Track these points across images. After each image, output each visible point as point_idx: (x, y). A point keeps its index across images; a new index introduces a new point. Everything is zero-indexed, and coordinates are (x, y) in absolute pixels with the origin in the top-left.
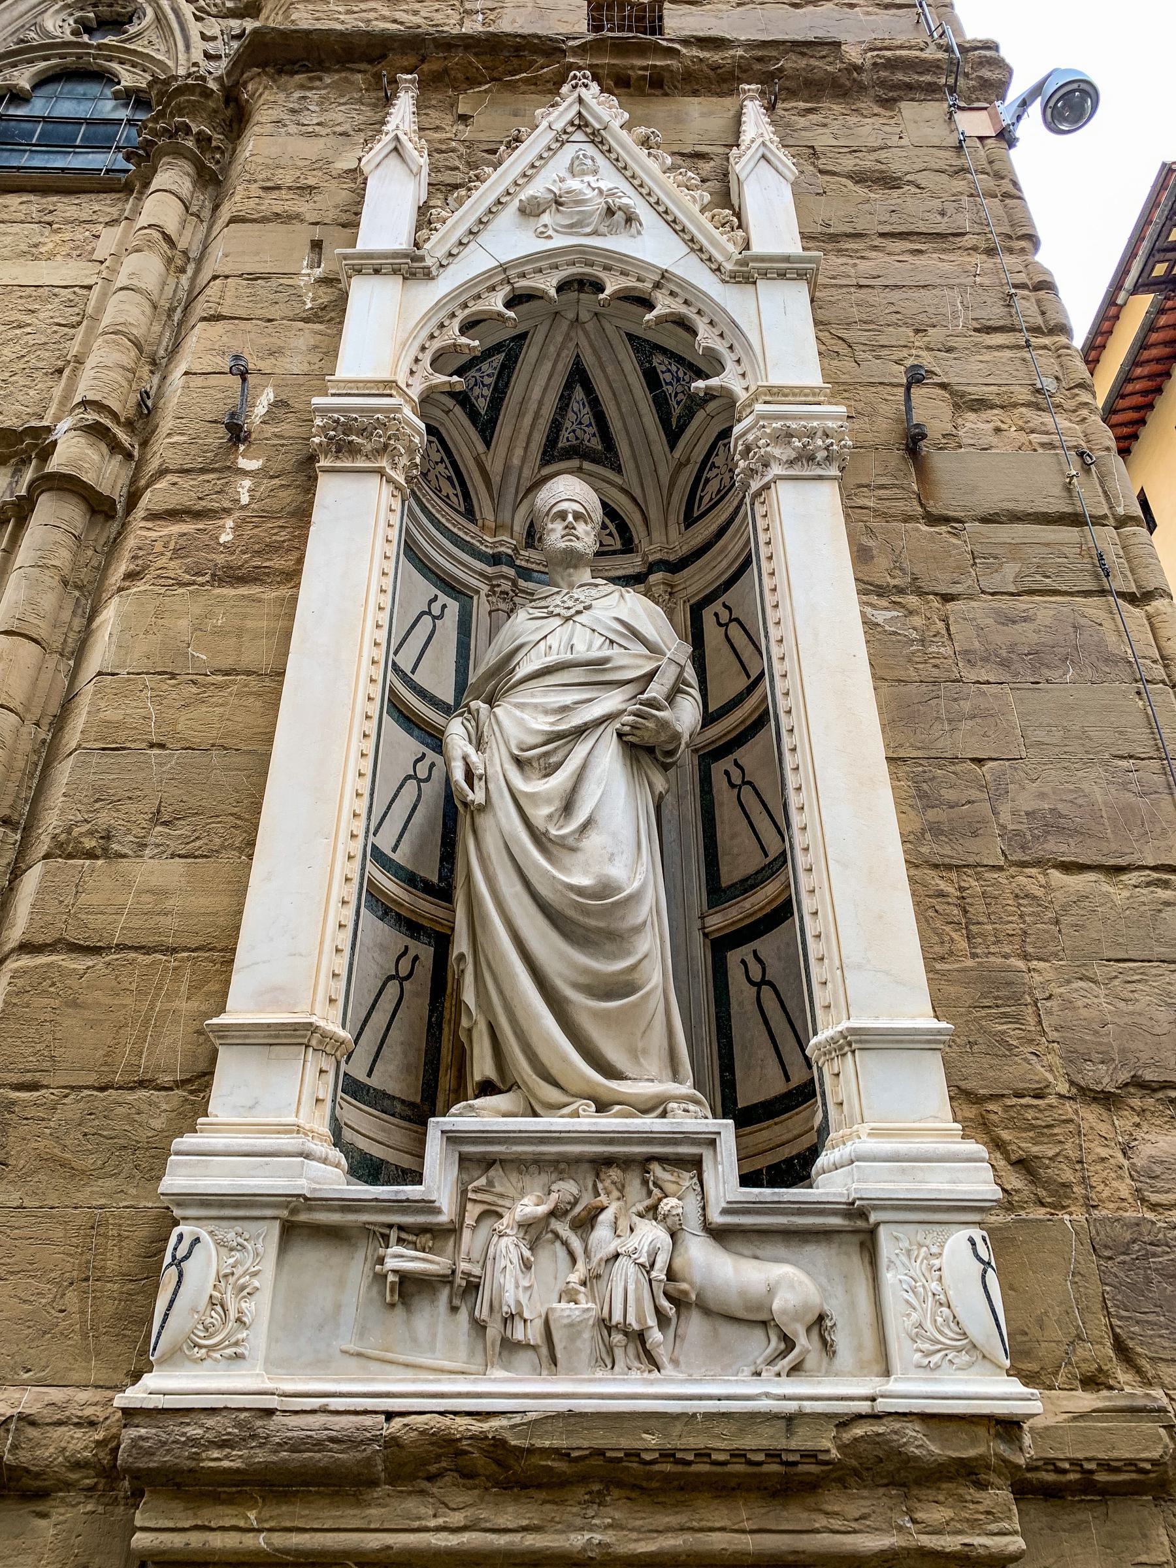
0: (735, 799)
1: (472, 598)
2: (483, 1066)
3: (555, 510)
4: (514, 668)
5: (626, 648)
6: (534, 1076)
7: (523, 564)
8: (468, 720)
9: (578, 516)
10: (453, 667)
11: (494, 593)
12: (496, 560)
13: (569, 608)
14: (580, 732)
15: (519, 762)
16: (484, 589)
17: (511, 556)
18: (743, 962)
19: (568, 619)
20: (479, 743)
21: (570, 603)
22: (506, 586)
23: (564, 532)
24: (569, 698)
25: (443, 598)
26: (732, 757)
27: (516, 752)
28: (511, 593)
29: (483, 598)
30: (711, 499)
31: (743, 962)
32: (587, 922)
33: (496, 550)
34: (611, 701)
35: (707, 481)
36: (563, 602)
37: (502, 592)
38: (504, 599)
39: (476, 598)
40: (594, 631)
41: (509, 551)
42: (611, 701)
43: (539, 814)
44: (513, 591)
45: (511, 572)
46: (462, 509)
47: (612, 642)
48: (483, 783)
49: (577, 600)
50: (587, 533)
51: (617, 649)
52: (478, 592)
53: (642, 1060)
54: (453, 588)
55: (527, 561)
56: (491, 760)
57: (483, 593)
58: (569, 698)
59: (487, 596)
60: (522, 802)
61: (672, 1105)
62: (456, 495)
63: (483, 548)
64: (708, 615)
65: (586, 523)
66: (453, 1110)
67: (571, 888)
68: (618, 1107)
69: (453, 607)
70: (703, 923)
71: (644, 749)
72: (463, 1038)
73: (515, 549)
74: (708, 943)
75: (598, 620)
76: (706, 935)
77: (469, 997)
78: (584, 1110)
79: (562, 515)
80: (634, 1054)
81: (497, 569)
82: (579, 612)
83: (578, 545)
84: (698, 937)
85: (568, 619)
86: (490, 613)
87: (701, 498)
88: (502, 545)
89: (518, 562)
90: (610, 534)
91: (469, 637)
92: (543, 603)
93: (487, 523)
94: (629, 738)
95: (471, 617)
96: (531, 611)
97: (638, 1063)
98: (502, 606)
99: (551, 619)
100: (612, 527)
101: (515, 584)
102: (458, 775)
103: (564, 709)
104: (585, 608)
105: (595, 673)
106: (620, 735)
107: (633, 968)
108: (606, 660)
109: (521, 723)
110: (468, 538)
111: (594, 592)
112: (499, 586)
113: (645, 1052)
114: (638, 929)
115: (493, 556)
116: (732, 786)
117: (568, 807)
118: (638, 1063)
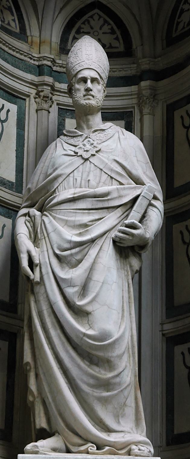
0: (185, 251)
1: (25, 100)
2: (41, 422)
3: (80, 76)
4: (55, 190)
5: (121, 184)
6: (66, 430)
7: (58, 69)
8: (28, 222)
9: (93, 80)
10: (14, 154)
11: (40, 96)
12: (40, 70)
13: (87, 151)
14: (93, 241)
15: (57, 256)
16: (33, 92)
17: (50, 67)
18: (183, 354)
19: (86, 160)
20: (35, 240)
21: (88, 147)
22: (47, 90)
23: (84, 93)
24: (86, 218)
25: (8, 105)
26: (185, 223)
27: (58, 252)
28: (50, 95)
29: (33, 100)
30: (184, 28)
31: (183, 354)
32: (93, 354)
33: (40, 63)
34: (111, 220)
35: (182, 11)
36: (84, 145)
37: (44, 97)
38: (46, 101)
39: (27, 99)
40: (101, 170)
41: (49, 63)
42: (111, 220)
43: (70, 291)
44: (52, 94)
45: (49, 80)
46: (18, 31)
47: (112, 178)
48: (38, 268)
49: (92, 144)
50: (99, 91)
51: (115, 186)
52: (28, 96)
53: (120, 420)
54: (14, 96)
55: (61, 67)
56: (42, 252)
57: (32, 96)
58: (86, 218)
59: (35, 98)
60: (61, 283)
61: (134, 447)
62: (14, 20)
63: (32, 61)
64: (177, 114)
65: (99, 83)
66: (29, 447)
67: (85, 335)
68: (107, 448)
69: (14, 108)
70: (162, 328)
71: (127, 249)
72: (29, 405)
73: (53, 61)
74: (165, 339)
75: (103, 162)
76: (163, 335)
77: (33, 385)
78: (91, 449)
79: (84, 80)
80: (117, 417)
81: (41, 78)
82: (93, 155)
83: (93, 102)
84: (159, 334)
85: (86, 160)
86: (37, 111)
87: (178, 23)
88: (44, 59)
89: (55, 68)
90: (117, 39)
91: (24, 130)
92: (72, 141)
93: (34, 39)
94: (118, 244)
95: (25, 115)
96: (65, 145)
97: (119, 422)
98: (45, 106)
99: (76, 158)
100: (118, 33)
101: (53, 88)
102: (25, 263)
103: (86, 226)
104: (97, 152)
105: (100, 202)
106: (114, 242)
107: (118, 375)
108: (107, 194)
109: (59, 234)
110: (22, 57)
111: (101, 135)
112: (42, 91)
113: (123, 416)
114: (120, 357)
115: (39, 66)
116: (184, 242)
117: (84, 289)
118: (119, 422)
